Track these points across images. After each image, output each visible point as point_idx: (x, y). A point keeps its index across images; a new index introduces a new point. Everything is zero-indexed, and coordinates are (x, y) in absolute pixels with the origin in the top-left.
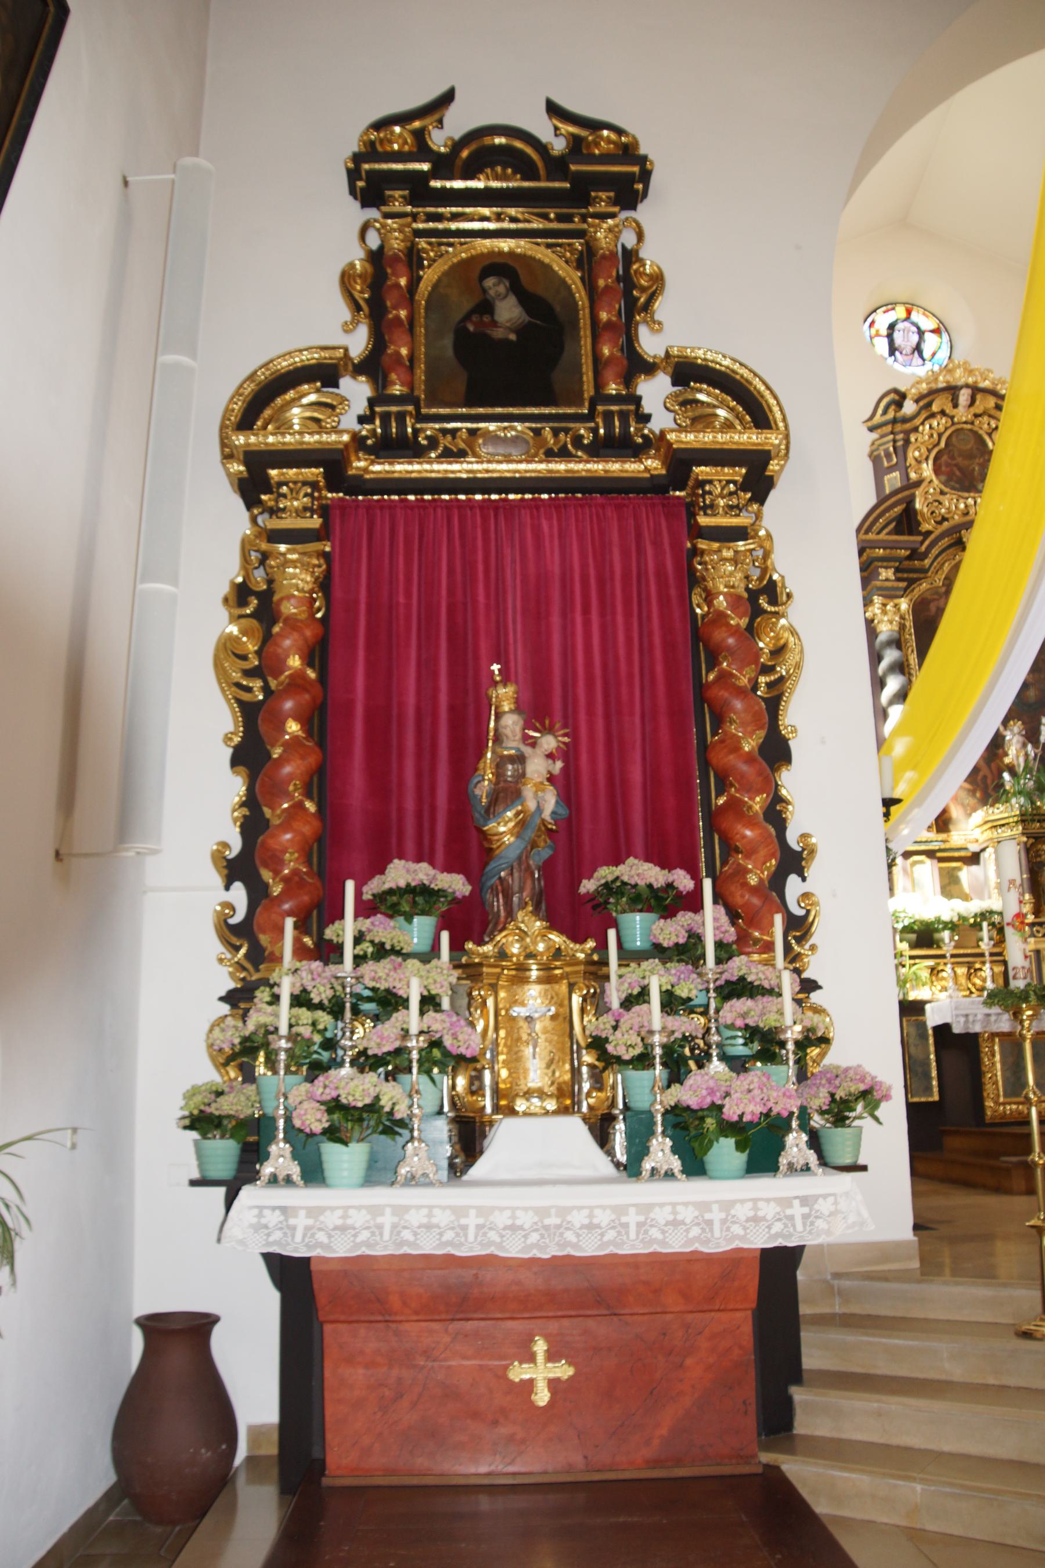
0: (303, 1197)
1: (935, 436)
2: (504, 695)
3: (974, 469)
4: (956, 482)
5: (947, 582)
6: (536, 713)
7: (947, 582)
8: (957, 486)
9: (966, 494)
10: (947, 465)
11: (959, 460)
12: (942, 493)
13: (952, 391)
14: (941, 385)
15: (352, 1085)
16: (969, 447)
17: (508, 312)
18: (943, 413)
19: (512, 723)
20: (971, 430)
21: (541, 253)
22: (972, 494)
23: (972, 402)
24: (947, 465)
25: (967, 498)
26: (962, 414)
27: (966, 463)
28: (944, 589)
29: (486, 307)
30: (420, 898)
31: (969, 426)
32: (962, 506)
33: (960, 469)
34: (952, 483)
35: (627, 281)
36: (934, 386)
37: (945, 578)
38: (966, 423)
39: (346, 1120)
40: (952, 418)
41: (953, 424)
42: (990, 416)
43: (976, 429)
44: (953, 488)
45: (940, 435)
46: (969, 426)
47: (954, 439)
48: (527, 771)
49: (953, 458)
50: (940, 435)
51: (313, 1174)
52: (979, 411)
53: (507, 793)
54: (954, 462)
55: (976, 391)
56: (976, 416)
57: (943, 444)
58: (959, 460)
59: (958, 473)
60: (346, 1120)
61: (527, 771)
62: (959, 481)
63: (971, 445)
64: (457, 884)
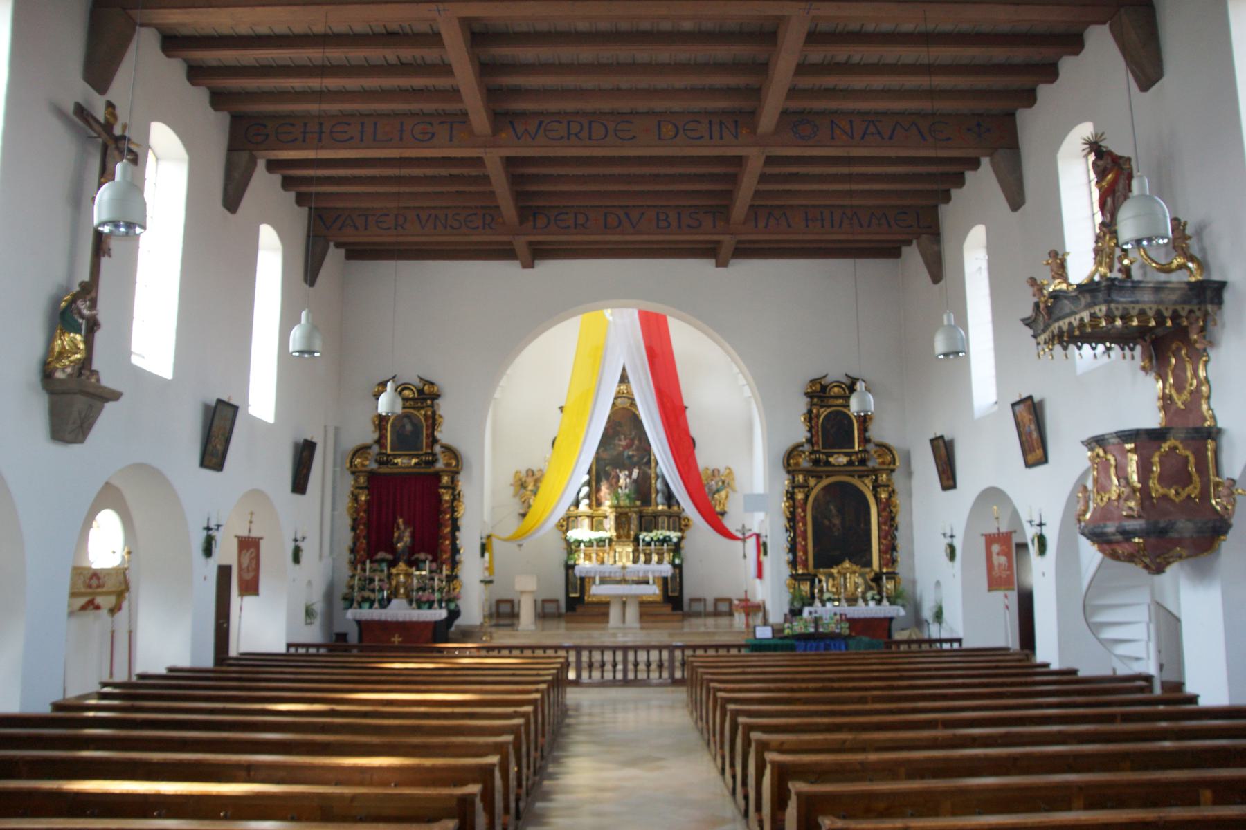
0: (359, 611)
2: (401, 521)
6: (407, 523)
15: (367, 594)
17: (409, 427)
19: (402, 527)
21: (415, 412)
29: (403, 426)
30: (382, 560)
35: (434, 420)
39: (365, 600)
48: (404, 539)
51: (360, 607)
53: (400, 539)
60: (365, 600)
61: (404, 539)
64: (390, 557)
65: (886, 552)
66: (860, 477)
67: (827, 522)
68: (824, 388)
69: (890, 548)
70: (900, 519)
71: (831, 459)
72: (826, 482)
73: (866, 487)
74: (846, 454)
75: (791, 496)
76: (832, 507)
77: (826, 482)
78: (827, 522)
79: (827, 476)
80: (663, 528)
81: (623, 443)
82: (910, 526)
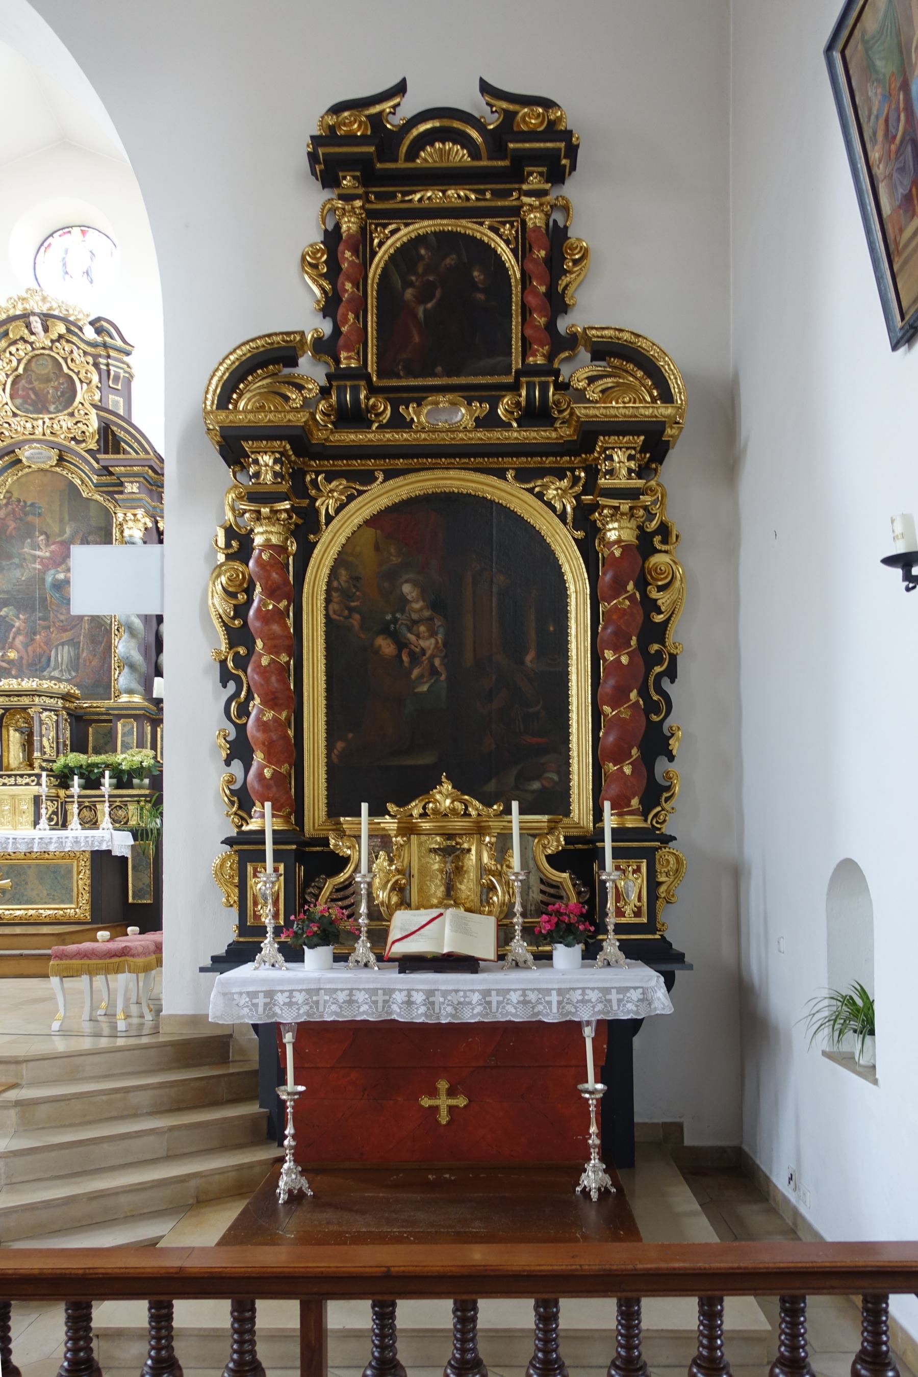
1: (15, 363)
3: (48, 392)
4: (30, 405)
5: (8, 495)
7: (8, 495)
8: (31, 408)
9: (35, 416)
10: (24, 389)
11: (36, 384)
12: (15, 415)
13: (25, 317)
14: (18, 312)
16: (46, 371)
18: (22, 338)
20: (49, 355)
22: (41, 416)
23: (46, 330)
24: (24, 389)
25: (36, 419)
26: (41, 339)
27: (42, 386)
28: (4, 501)
31: (47, 352)
32: (29, 425)
33: (36, 394)
34: (27, 406)
36: (12, 313)
37: (7, 492)
38: (43, 348)
40: (31, 344)
41: (33, 349)
42: (68, 341)
43: (52, 354)
44: (27, 411)
45: (19, 361)
46: (47, 352)
47: (33, 364)
49: (30, 382)
50: (19, 361)
52: (55, 336)
54: (31, 386)
55: (47, 319)
56: (52, 341)
57: (20, 370)
58: (36, 384)
59: (33, 396)
62: (34, 404)
63: (47, 369)
65: (619, 757)
66: (523, 476)
67: (386, 646)
68: (384, 138)
69: (644, 745)
70: (688, 636)
71: (410, 412)
72: (382, 495)
73: (543, 510)
74: (470, 393)
75: (239, 544)
76: (407, 588)
77: (382, 495)
78: (386, 646)
79: (390, 475)
80: (126, 747)
81: (44, 553)
82: (729, 661)
